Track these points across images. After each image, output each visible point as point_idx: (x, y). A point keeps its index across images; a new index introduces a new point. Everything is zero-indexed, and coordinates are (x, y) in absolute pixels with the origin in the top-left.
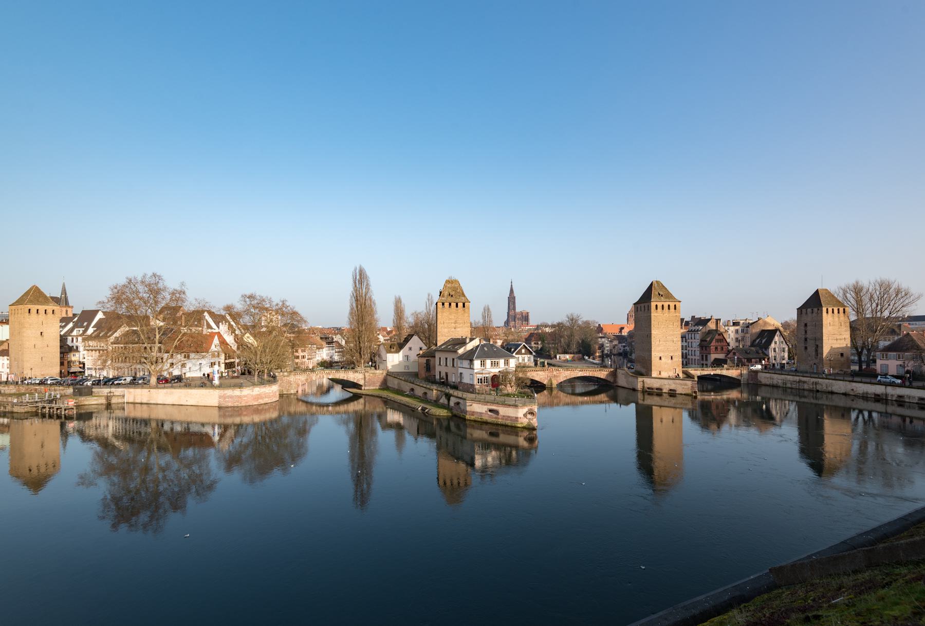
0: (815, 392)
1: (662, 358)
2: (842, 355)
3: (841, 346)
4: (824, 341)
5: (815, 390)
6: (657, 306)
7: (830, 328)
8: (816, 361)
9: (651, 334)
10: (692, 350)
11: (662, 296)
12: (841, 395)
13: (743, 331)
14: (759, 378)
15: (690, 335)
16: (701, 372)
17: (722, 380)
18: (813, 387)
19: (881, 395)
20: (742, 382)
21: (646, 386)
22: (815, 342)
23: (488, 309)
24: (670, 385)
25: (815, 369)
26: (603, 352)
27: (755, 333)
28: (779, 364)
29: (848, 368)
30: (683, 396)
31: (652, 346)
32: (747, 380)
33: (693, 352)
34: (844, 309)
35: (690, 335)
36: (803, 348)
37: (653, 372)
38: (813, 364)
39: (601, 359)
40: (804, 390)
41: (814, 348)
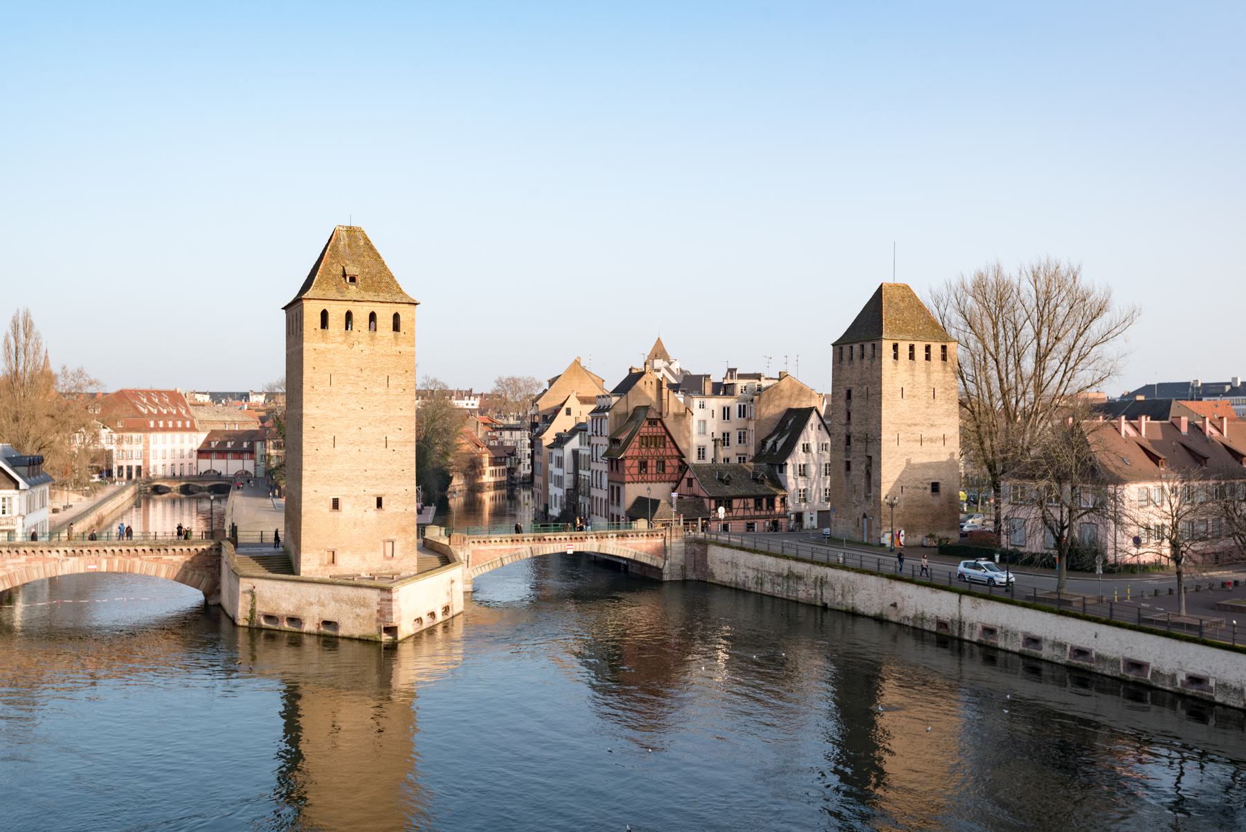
0: (819, 610)
1: (342, 504)
2: (935, 487)
3: (934, 459)
4: (885, 446)
5: (819, 604)
6: (324, 315)
7: (903, 405)
8: (867, 507)
9: (301, 415)
10: (597, 471)
11: (353, 279)
12: (872, 622)
13: (742, 412)
14: (709, 563)
15: (595, 421)
16: (536, 545)
17: (629, 570)
18: (816, 595)
19: (950, 627)
20: (666, 578)
21: (261, 608)
22: (866, 451)
23: (28, 326)
24: (323, 605)
25: (865, 533)
26: (511, 471)
27: (768, 419)
28: (815, 516)
29: (951, 529)
30: (356, 644)
31: (304, 459)
32: (684, 568)
33: (599, 478)
34: (944, 348)
35: (595, 421)
36: (844, 465)
37: (304, 557)
38: (861, 516)
39: (504, 492)
40: (797, 602)
41: (863, 467)
